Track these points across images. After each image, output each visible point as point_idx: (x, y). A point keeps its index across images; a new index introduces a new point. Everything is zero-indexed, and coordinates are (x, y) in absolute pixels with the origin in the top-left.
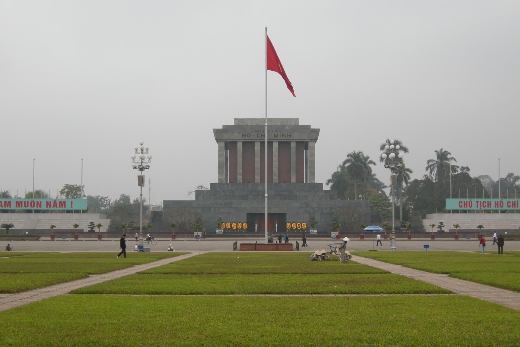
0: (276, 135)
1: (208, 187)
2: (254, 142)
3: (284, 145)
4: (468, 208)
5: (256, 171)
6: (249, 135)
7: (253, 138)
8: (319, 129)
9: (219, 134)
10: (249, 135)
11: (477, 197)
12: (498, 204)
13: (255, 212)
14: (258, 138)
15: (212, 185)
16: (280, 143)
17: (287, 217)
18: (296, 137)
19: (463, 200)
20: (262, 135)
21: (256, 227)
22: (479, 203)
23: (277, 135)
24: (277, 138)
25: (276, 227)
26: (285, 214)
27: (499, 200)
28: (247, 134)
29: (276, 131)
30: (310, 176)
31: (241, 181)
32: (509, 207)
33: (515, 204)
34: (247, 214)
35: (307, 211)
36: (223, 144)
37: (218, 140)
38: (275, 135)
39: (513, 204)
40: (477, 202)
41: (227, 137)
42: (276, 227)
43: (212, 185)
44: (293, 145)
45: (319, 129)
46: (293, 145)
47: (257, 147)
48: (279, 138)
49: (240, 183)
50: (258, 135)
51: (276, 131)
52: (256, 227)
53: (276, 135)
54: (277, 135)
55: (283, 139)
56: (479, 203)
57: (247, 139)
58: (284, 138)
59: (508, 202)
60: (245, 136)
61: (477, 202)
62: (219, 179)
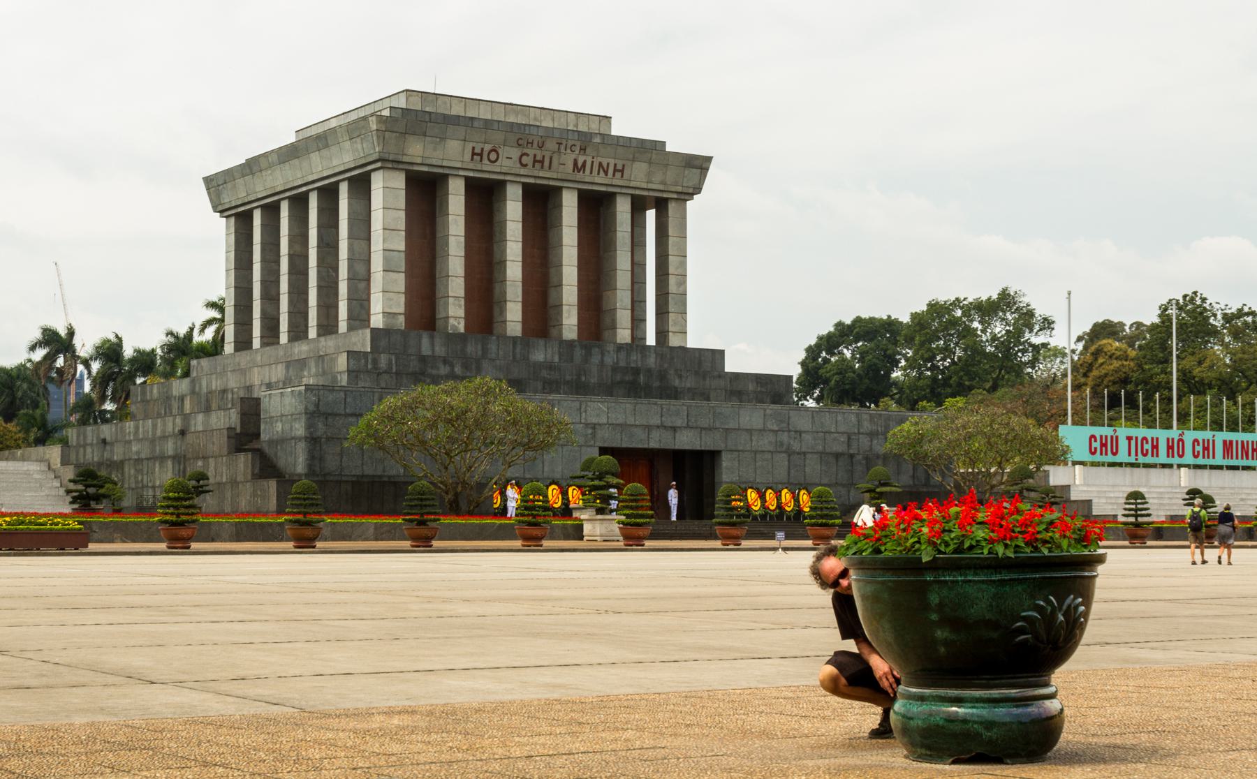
0: (580, 165)
1: (905, 319)
2: (502, 184)
3: (595, 207)
4: (1110, 458)
7: (507, 163)
8: (709, 159)
10: (493, 157)
11: (1092, 424)
12: (1172, 447)
14: (523, 171)
17: (724, 464)
19: (1100, 431)
20: (535, 161)
22: (1133, 442)
24: (579, 176)
26: (714, 455)
27: (1174, 433)
28: (487, 147)
31: (461, 328)
32: (1196, 456)
33: (1208, 449)
35: (782, 444)
39: (1204, 449)
40: (1129, 439)
41: (418, 152)
45: (709, 159)
46: (623, 208)
47: (513, 209)
51: (583, 150)
53: (580, 165)
55: (598, 181)
56: (1133, 442)
57: (487, 170)
58: (601, 179)
59: (1196, 441)
60: (481, 155)
61: (1129, 439)
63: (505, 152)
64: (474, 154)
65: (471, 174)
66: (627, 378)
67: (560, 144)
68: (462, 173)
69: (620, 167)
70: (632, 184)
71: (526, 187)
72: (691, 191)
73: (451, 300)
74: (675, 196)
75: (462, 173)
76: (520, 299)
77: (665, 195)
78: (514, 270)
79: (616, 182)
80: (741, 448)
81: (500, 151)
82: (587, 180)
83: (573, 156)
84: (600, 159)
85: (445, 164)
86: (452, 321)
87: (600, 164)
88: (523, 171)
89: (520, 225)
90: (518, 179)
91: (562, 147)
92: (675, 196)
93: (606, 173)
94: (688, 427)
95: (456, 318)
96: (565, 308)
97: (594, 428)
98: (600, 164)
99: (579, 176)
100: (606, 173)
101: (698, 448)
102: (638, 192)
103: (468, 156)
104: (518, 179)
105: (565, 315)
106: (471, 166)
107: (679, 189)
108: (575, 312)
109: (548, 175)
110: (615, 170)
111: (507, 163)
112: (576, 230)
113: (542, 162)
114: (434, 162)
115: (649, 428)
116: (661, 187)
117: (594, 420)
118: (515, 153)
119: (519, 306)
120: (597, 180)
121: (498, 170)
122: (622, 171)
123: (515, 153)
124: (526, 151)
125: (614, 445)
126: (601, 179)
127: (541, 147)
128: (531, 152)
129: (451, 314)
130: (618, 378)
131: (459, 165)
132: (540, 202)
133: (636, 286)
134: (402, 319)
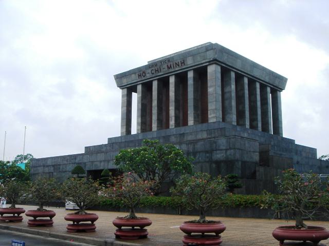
0: (169, 66)
3: (182, 79)
9: (119, 78)
15: (109, 139)
16: (177, 76)
18: (190, 62)
20: (156, 71)
23: (171, 66)
28: (142, 72)
30: (211, 114)
36: (126, 90)
37: (121, 87)
38: (168, 67)
41: (125, 81)
43: (109, 139)
50: (153, 72)
53: (169, 66)
60: (140, 75)
62: (122, 133)
64: (139, 76)
65: (142, 82)
67: (161, 62)
68: (139, 83)
70: (189, 66)
71: (158, 80)
72: (212, 59)
74: (207, 64)
75: (139, 83)
77: (204, 65)
82: (173, 70)
87: (176, 63)
92: (207, 64)
93: (178, 65)
98: (176, 63)
99: (171, 70)
100: (178, 65)
102: (193, 68)
103: (138, 78)
107: (207, 61)
108: (173, 118)
109: (160, 74)
113: (158, 70)
115: (101, 162)
116: (200, 63)
120: (177, 69)
122: (184, 63)
123: (149, 71)
127: (156, 65)
128: (153, 68)
132: (164, 83)
133: (227, 102)
134: (125, 133)
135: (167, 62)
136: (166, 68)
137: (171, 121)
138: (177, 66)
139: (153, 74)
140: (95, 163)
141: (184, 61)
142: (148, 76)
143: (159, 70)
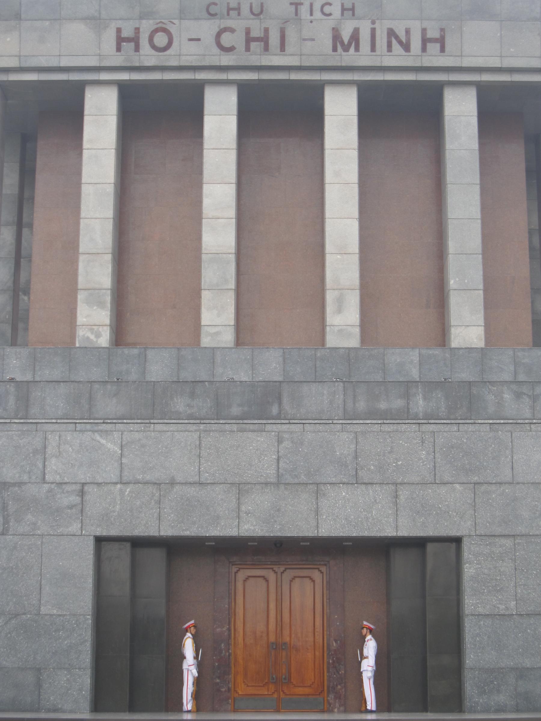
0: (346, 37)
5: (210, 275)
6: (161, 40)
10: (161, 40)
13: (167, 531)
17: (469, 570)
20: (249, 40)
21: (190, 670)
23: (355, 37)
25: (368, 666)
28: (147, 26)
29: (349, 11)
34: (99, 540)
38: (336, 37)
42: (368, 666)
44: (461, 112)
48: (363, 57)
49: (91, 350)
50: (227, 40)
52: (190, 670)
53: (346, 37)
54: (355, 37)
60: (135, 40)
63: (182, 30)
64: (120, 40)
65: (125, 76)
66: (383, 405)
67: (297, 5)
68: (104, 76)
69: (433, 33)
70: (467, 62)
73: (81, 296)
75: (104, 76)
76: (232, 285)
78: (219, 235)
79: (427, 62)
80: (521, 529)
81: (173, 30)
83: (330, 23)
84: (388, 24)
85: (65, 62)
86: (82, 334)
87: (391, 33)
88: (226, 60)
89: (232, 157)
90: (223, 76)
91: (304, 10)
93: (406, 47)
94: (357, 481)
95: (91, 327)
96: (330, 296)
97: (82, 493)
98: (391, 33)
99: (350, 58)
100: (406, 47)
101: (389, 532)
102: (486, 77)
104: (223, 76)
105: (330, 309)
106: (118, 60)
108: (353, 301)
110: (425, 41)
111: (193, 48)
112: (355, 154)
113: (265, 40)
114: (44, 62)
115: (241, 489)
117: (82, 477)
118: (207, 29)
119: (230, 300)
120: (389, 61)
121: (174, 63)
122: (441, 41)
123: (207, 29)
124: (229, 23)
125: (139, 531)
126: (397, 58)
127: (259, 13)
128: (238, 24)
129: (81, 319)
130: (362, 405)
131: (93, 62)
135: (336, 10)
136: (328, 43)
137: (339, 310)
138: (397, 48)
139: (231, 49)
140: (192, 491)
141: (442, 30)
142: (184, 52)
143: (274, 39)
